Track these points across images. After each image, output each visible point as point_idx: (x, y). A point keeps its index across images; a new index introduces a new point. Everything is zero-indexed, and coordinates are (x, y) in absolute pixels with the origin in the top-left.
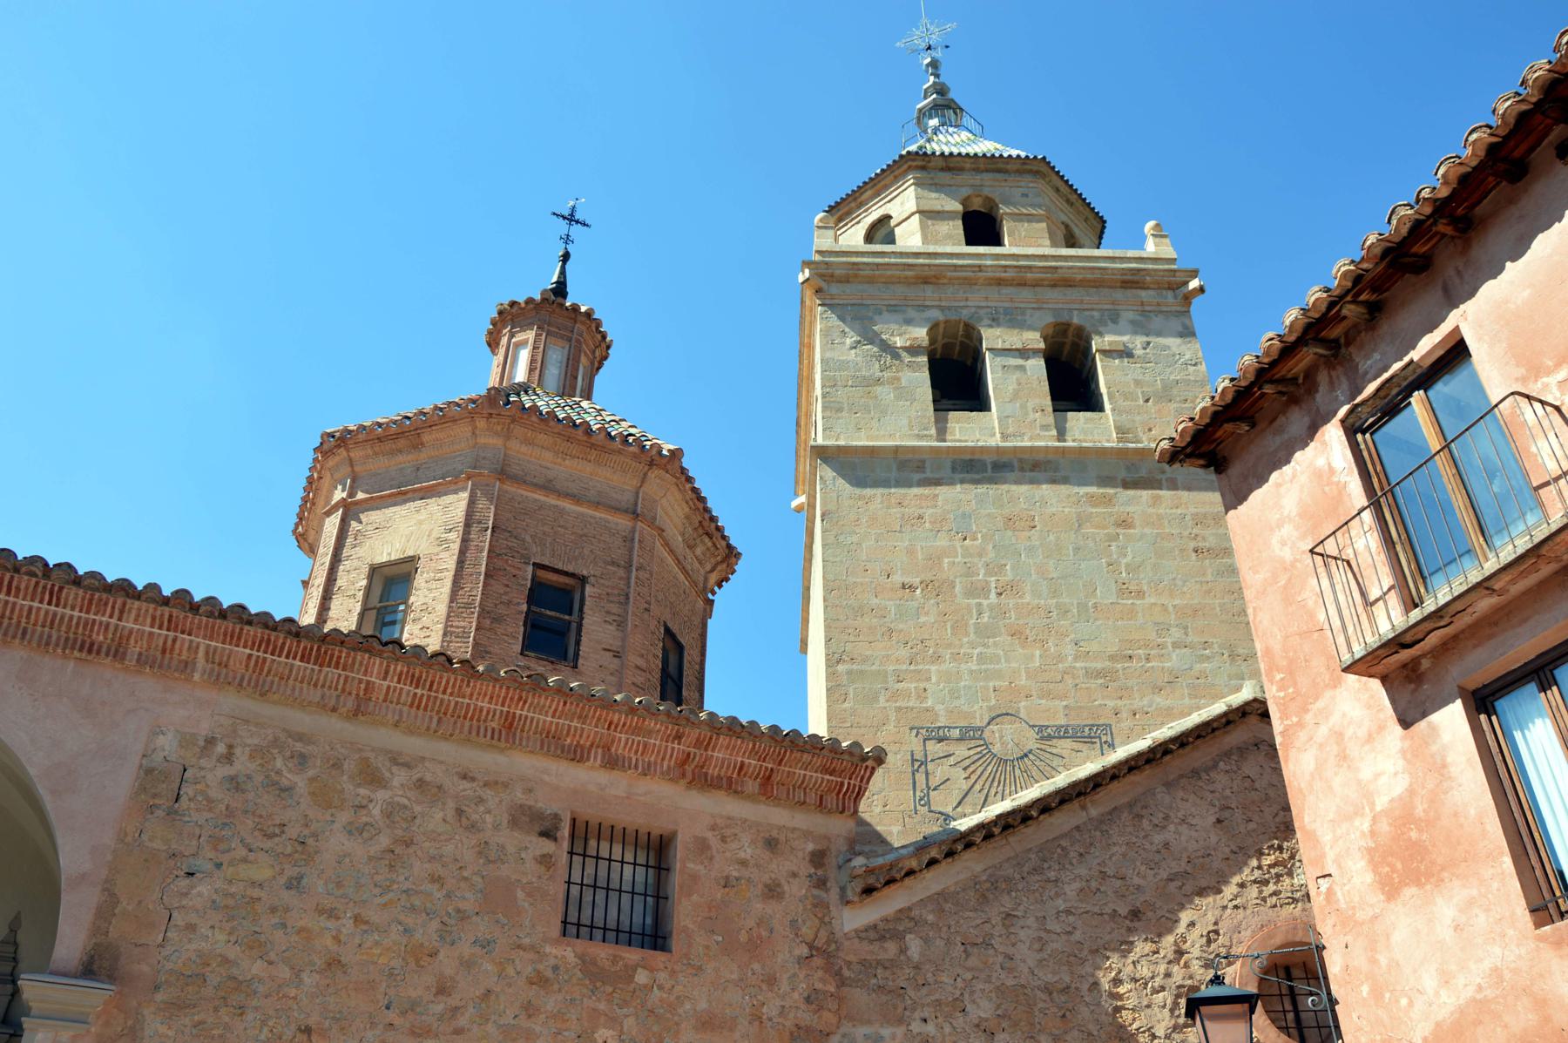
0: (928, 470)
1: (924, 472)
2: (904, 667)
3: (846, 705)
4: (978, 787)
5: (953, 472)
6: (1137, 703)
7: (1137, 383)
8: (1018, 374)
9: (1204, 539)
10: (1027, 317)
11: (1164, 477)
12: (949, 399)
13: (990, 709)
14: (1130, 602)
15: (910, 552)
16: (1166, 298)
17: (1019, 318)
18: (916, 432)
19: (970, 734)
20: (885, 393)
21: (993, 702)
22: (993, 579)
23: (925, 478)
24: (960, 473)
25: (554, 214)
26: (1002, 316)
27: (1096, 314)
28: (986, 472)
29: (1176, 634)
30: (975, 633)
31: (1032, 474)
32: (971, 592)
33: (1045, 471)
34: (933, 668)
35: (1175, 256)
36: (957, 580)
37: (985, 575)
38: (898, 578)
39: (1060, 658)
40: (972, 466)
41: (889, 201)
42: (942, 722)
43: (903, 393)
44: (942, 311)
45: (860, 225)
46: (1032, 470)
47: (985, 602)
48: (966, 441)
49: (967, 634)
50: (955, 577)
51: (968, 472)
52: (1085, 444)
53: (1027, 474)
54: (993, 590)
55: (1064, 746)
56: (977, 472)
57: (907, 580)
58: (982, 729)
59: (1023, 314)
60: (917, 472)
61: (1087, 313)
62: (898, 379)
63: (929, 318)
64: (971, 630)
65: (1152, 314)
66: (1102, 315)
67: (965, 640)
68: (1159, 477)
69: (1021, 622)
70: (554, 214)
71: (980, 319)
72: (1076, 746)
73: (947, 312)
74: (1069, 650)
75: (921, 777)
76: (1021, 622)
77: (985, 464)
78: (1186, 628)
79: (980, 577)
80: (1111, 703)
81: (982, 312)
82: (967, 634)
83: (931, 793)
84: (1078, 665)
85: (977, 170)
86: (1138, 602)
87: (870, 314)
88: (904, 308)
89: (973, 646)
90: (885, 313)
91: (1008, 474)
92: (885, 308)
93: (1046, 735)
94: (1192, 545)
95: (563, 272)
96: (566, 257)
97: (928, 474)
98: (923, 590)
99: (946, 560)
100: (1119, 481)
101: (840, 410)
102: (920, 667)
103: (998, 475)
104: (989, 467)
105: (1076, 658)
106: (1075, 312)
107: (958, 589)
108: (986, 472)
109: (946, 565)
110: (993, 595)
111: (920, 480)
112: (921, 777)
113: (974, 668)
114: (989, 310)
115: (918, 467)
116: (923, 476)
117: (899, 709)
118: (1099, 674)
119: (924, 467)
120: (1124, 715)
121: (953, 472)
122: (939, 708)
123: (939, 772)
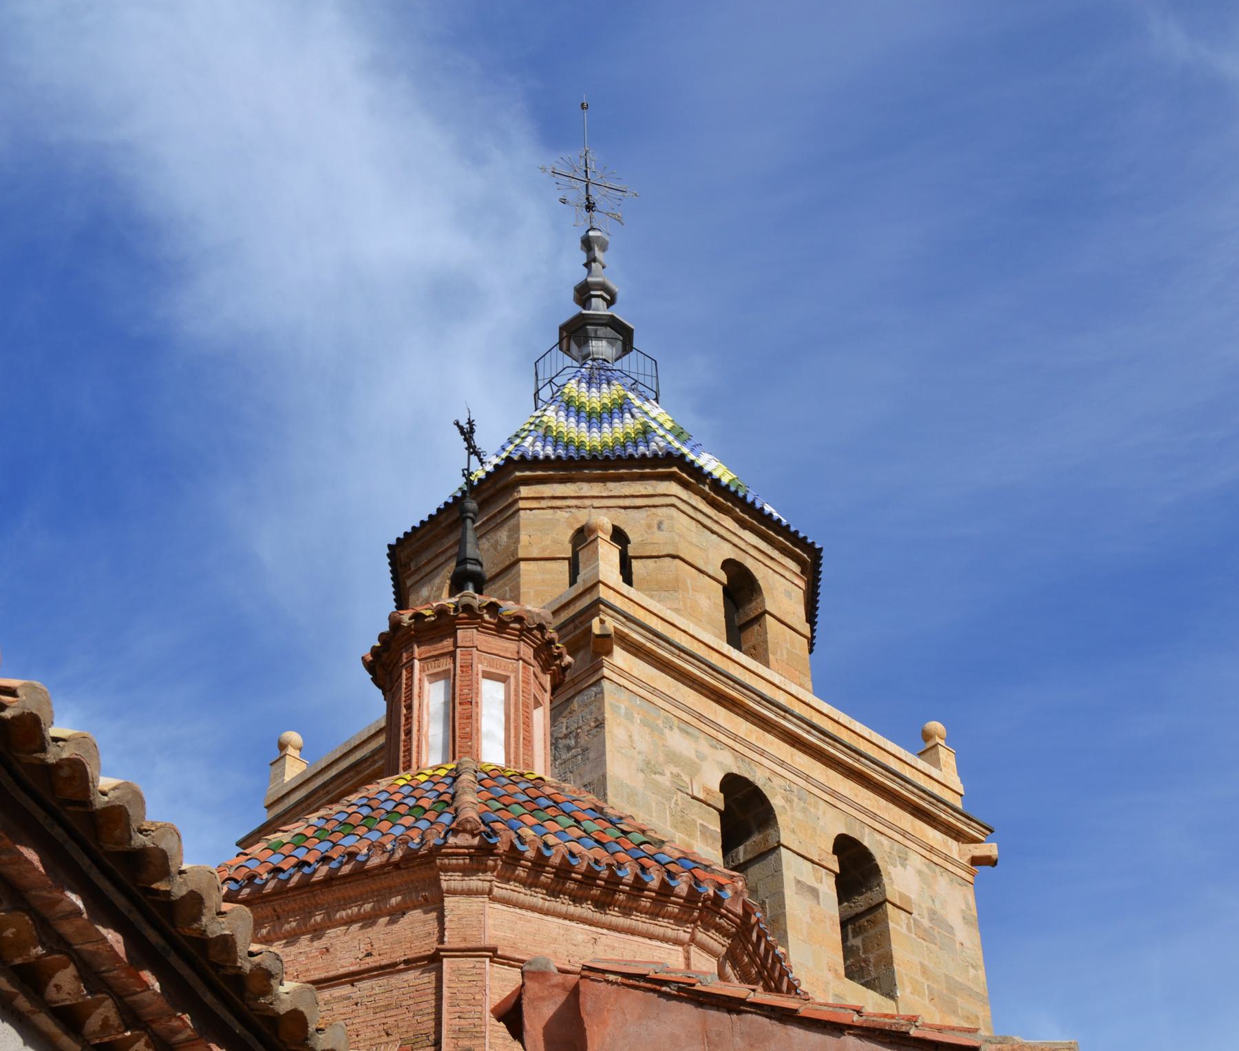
7: (925, 971)
8: (808, 902)
10: (820, 813)
26: (796, 800)
35: (962, 793)
41: (625, 508)
61: (878, 836)
63: (721, 763)
65: (938, 869)
73: (740, 764)
81: (777, 781)
87: (660, 722)
88: (697, 733)
90: (676, 730)
106: (867, 830)
114: (782, 782)
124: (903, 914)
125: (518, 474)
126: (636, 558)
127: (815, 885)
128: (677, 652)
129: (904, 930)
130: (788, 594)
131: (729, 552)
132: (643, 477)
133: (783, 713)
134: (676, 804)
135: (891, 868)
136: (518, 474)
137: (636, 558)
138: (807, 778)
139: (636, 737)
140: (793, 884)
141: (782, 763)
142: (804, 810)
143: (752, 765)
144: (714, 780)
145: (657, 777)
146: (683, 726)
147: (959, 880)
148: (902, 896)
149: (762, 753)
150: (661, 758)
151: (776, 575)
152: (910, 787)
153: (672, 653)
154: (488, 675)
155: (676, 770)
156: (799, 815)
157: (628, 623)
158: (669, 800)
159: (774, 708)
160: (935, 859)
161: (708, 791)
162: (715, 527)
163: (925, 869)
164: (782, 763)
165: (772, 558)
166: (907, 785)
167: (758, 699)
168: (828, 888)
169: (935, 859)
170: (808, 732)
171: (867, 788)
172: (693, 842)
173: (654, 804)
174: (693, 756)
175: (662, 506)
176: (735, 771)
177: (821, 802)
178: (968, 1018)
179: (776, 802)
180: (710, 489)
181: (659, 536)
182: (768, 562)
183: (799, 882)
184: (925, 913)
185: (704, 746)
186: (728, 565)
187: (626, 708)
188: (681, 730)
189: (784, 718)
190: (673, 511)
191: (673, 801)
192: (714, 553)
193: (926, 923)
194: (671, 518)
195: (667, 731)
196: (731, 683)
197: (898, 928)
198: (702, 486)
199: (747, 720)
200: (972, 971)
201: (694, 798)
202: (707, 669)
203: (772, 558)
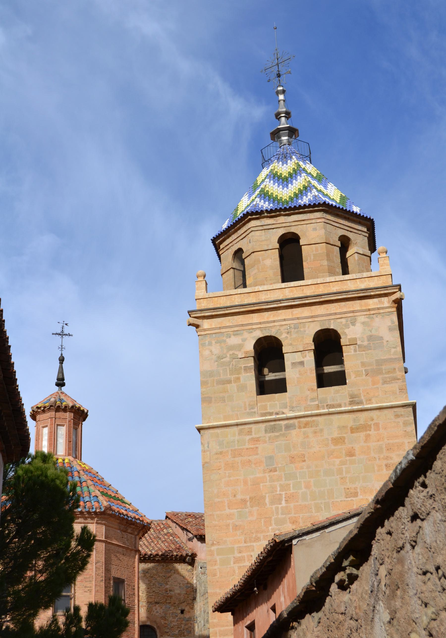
0: (253, 433)
1: (251, 435)
2: (242, 545)
3: (216, 567)
5: (266, 433)
7: (363, 364)
8: (300, 368)
9: (391, 458)
11: (372, 423)
12: (273, 372)
14: (349, 499)
15: (245, 482)
16: (383, 303)
17: (302, 330)
20: (232, 387)
22: (283, 493)
23: (252, 438)
24: (269, 433)
25: (53, 334)
27: (343, 320)
28: (282, 431)
30: (275, 524)
31: (305, 429)
32: (272, 502)
33: (312, 427)
34: (254, 544)
36: (267, 495)
37: (280, 491)
38: (239, 497)
40: (275, 428)
41: (242, 239)
43: (242, 388)
44: (262, 331)
45: (230, 250)
46: (304, 427)
47: (280, 506)
49: (271, 525)
50: (266, 493)
51: (273, 432)
52: (331, 410)
53: (303, 430)
54: (284, 499)
57: (243, 497)
59: (304, 327)
60: (248, 435)
61: (339, 320)
62: (238, 379)
64: (273, 522)
66: (347, 321)
67: (270, 528)
68: (369, 423)
69: (297, 515)
70: (53, 334)
71: (281, 334)
73: (264, 331)
76: (297, 515)
77: (281, 427)
79: (278, 493)
81: (282, 328)
82: (271, 525)
86: (354, 499)
87: (225, 338)
88: (242, 332)
90: (232, 337)
91: (292, 431)
92: (232, 333)
94: (385, 462)
95: (61, 370)
96: (62, 360)
97: (254, 436)
98: (250, 502)
99: (261, 484)
100: (349, 428)
101: (210, 402)
102: (249, 544)
103: (288, 432)
104: (283, 428)
107: (267, 501)
108: (282, 431)
109: (261, 487)
110: (283, 502)
111: (249, 440)
114: (286, 327)
115: (248, 432)
116: (251, 437)
119: (251, 432)
121: (266, 433)
124: (352, 347)
125: (217, 242)
126: (245, 258)
127: (302, 360)
128: (225, 309)
129: (353, 352)
130: (315, 229)
132: (244, 224)
133: (279, 302)
134: (233, 365)
135: (346, 331)
136: (217, 242)
137: (245, 258)
139: (213, 350)
143: (270, 329)
144: (250, 347)
145: (224, 360)
146: (236, 333)
147: (388, 314)
148: (350, 340)
149: (274, 321)
150: (225, 351)
151: (308, 225)
152: (351, 293)
153: (224, 310)
154: (43, 427)
155: (231, 352)
157: (202, 312)
158: (230, 365)
159: (275, 303)
160: (372, 312)
161: (246, 353)
163: (367, 320)
166: (349, 293)
167: (266, 304)
169: (372, 312)
170: (294, 302)
171: (333, 303)
172: (240, 376)
173: (221, 371)
174: (240, 342)
175: (250, 233)
176: (261, 336)
178: (389, 372)
179: (282, 337)
180: (267, 214)
182: (303, 223)
183: (293, 364)
184: (366, 339)
185: (246, 335)
187: (209, 342)
188: (234, 335)
189: (281, 303)
190: (253, 233)
191: (231, 366)
193: (366, 343)
194: (252, 236)
195: (228, 340)
196: (252, 305)
197: (350, 354)
198: (263, 215)
199: (268, 311)
200: (393, 350)
201: (240, 358)
202: (240, 307)
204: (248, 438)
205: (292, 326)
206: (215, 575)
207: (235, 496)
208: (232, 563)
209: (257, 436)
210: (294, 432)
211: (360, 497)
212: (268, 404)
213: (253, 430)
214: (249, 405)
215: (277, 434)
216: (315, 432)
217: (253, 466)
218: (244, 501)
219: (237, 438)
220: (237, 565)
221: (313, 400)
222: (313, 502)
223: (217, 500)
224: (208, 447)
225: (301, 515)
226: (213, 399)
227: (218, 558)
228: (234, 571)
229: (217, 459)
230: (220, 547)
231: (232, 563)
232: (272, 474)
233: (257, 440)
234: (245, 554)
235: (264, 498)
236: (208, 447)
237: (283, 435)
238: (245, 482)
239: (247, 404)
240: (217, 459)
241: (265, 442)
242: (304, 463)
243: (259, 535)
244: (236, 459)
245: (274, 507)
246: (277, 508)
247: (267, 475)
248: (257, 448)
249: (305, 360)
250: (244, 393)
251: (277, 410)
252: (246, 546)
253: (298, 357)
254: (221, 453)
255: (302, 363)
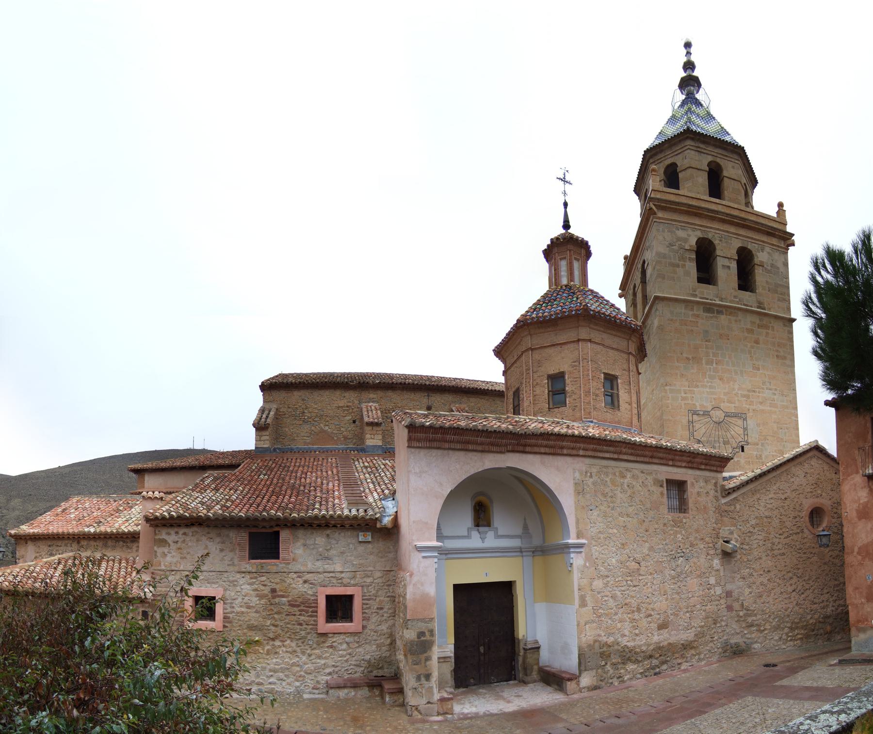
3: (669, 402)
4: (708, 431)
6: (754, 407)
13: (712, 405)
15: (689, 345)
18: (691, 292)
19: (706, 414)
21: (713, 403)
29: (768, 384)
33: (734, 316)
34: (695, 389)
38: (685, 355)
39: (734, 389)
41: (676, 155)
42: (698, 409)
43: (687, 274)
47: (712, 367)
48: (707, 299)
55: (733, 420)
56: (711, 313)
58: (709, 412)
64: (707, 376)
67: (705, 380)
72: (736, 419)
74: (736, 387)
75: (691, 427)
78: (770, 383)
80: (747, 406)
81: (716, 236)
83: (695, 433)
84: (739, 392)
85: (716, 146)
89: (708, 382)
93: (727, 415)
97: (695, 312)
105: (738, 390)
107: (704, 362)
111: (692, 315)
112: (691, 427)
113: (708, 390)
114: (718, 235)
117: (685, 404)
118: (744, 396)
120: (751, 410)
122: (697, 404)
123: (697, 426)
131: (710, 159)
138: (727, 232)
140: (721, 267)
141: (718, 229)
142: (726, 242)
156: (724, 244)
162: (705, 151)
164: (718, 229)
165: (727, 156)
168: (734, 265)
177: (733, 239)
179: (716, 242)
181: (686, 161)
183: (723, 265)
186: (709, 164)
192: (704, 161)
203: (727, 156)
204: (691, 313)
205: (723, 236)
206: (668, 407)
207: (682, 354)
208: (680, 400)
209: (698, 313)
210: (723, 317)
211: (761, 371)
212: (705, 291)
213: (695, 308)
214: (692, 288)
215: (711, 315)
216: (736, 321)
217: (694, 334)
218: (688, 359)
219: (683, 311)
220: (683, 402)
221: (735, 297)
222: (733, 368)
223: (669, 354)
224: (662, 313)
225: (726, 375)
226: (666, 277)
227: (670, 395)
228: (681, 406)
229: (669, 324)
230: (672, 388)
231: (680, 400)
232: (707, 343)
233: (698, 316)
234: (689, 395)
235: (701, 359)
236: (662, 313)
237: (716, 317)
238: (689, 345)
239: (691, 287)
240: (669, 324)
241: (703, 319)
242: (728, 341)
243: (698, 384)
244: (683, 327)
245: (708, 366)
246: (710, 368)
247: (704, 343)
248: (697, 322)
249: (731, 265)
250: (689, 278)
251: (711, 298)
252: (689, 390)
253: (726, 262)
254: (672, 320)
255: (729, 267)
